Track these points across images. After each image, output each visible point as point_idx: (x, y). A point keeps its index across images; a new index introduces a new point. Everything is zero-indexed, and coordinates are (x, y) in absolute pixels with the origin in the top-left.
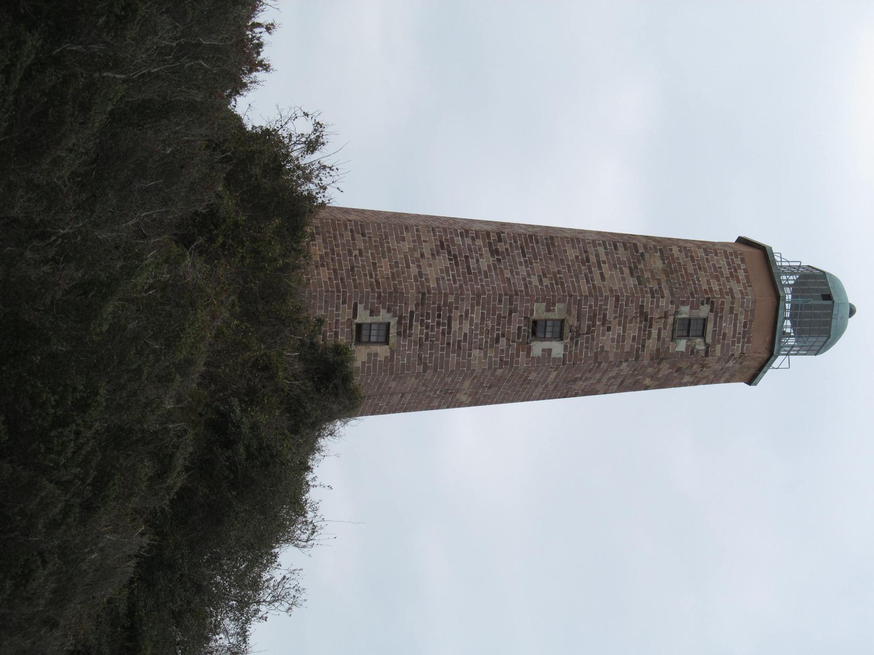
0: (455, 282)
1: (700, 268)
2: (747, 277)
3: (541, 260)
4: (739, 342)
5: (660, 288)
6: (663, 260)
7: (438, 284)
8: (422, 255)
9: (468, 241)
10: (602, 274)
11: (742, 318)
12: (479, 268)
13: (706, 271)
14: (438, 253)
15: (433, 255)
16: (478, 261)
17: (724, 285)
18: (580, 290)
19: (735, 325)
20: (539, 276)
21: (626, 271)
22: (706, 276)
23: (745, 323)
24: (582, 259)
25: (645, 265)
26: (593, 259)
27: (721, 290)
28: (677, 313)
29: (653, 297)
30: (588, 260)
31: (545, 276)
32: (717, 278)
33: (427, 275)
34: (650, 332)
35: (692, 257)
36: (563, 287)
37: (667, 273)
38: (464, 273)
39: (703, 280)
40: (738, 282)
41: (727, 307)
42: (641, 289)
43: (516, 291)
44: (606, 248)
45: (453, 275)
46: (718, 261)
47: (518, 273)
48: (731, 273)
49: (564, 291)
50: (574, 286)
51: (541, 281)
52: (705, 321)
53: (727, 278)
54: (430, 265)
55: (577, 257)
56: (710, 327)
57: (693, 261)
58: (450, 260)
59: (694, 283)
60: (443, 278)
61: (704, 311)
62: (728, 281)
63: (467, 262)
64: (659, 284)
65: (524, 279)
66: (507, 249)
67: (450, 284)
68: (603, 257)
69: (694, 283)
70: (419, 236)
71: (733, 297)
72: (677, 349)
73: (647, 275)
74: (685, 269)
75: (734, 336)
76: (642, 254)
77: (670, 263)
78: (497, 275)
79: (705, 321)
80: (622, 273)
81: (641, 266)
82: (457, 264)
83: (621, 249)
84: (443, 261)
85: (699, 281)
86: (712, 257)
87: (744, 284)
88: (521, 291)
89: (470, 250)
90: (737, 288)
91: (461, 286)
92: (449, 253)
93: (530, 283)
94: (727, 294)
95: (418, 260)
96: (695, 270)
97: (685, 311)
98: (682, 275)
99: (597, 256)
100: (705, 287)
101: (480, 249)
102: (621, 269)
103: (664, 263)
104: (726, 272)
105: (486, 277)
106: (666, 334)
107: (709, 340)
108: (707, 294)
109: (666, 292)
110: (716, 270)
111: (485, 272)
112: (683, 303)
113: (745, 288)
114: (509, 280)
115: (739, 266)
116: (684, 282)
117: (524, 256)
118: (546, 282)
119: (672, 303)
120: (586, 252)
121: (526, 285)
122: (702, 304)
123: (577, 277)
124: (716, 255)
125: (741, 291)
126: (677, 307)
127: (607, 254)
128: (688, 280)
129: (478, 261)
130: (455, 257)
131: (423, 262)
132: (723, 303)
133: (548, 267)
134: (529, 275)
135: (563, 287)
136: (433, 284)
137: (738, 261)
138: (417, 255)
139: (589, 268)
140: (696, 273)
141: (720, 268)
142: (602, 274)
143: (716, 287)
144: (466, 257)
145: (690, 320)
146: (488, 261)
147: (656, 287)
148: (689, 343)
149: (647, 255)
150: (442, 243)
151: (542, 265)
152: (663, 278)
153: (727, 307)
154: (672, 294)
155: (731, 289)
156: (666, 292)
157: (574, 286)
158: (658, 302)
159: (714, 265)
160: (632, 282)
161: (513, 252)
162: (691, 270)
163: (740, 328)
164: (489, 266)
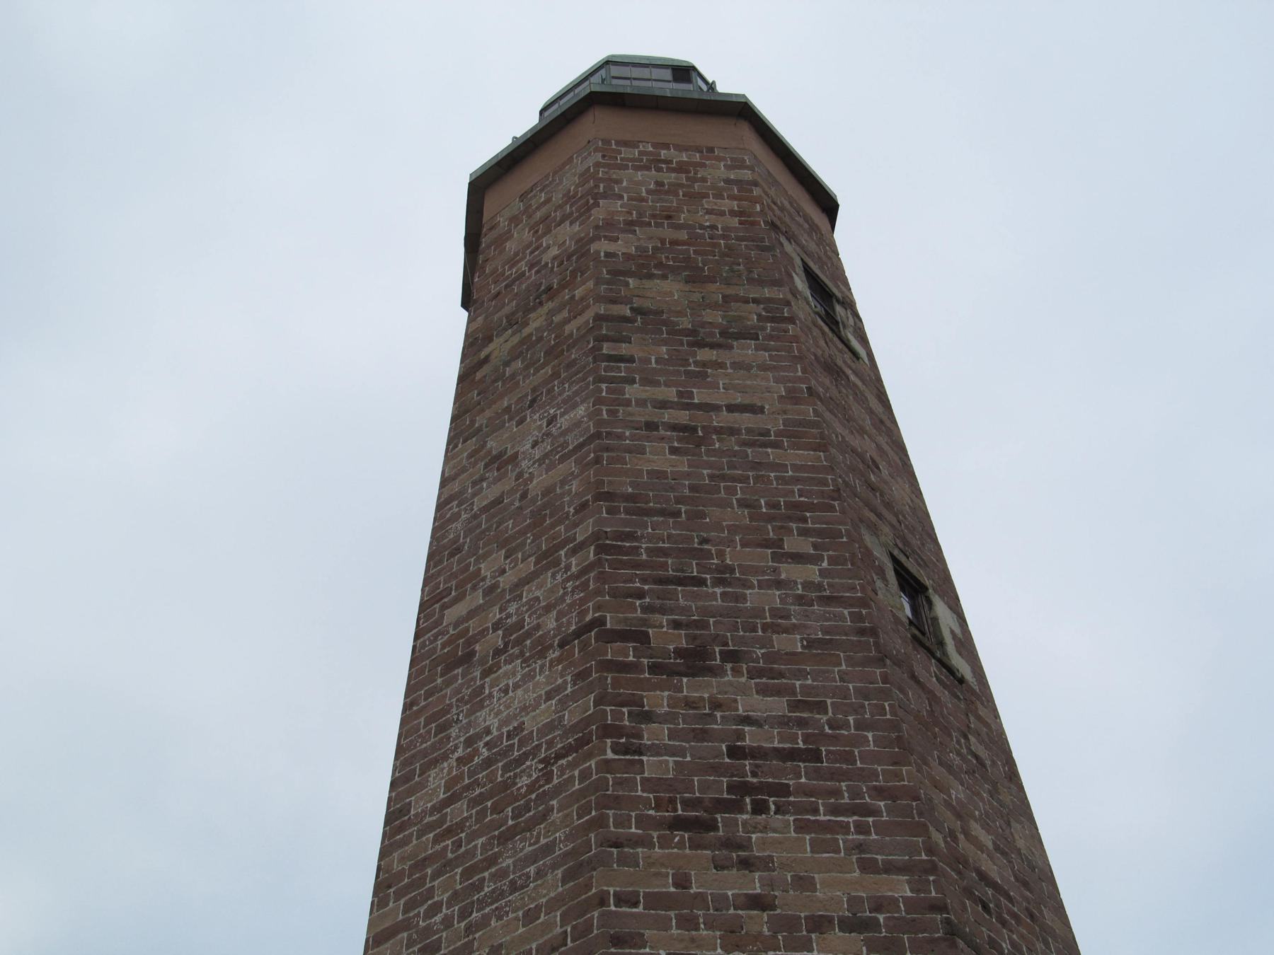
0: (875, 812)
1: (669, 217)
2: (679, 148)
3: (704, 541)
5: (755, 301)
6: (650, 276)
7: (889, 868)
8: (757, 903)
9: (652, 734)
10: (731, 408)
11: (786, 203)
12: (783, 722)
13: (679, 210)
14: (743, 845)
15: (746, 864)
16: (747, 720)
18: (813, 469)
20: (777, 557)
21: (705, 354)
24: (680, 440)
25: (680, 313)
26: (683, 417)
27: (732, 198)
29: (791, 320)
30: (688, 429)
31: (778, 543)
32: (695, 197)
33: (853, 901)
35: (631, 223)
36: (811, 507)
38: (817, 774)
42: (771, 337)
43: (862, 632)
44: (633, 381)
45: (835, 810)
46: (639, 183)
47: (775, 613)
48: (670, 170)
49: (832, 509)
50: (797, 480)
51: (798, 558)
54: (803, 883)
55: (674, 451)
57: (649, 224)
58: (760, 808)
60: (860, 847)
63: (755, 753)
64: (746, 301)
65: (800, 600)
66: (677, 625)
67: (880, 829)
68: (671, 394)
70: (656, 901)
74: (674, 243)
77: (660, 265)
78: (802, 674)
80: (722, 365)
81: (685, 323)
82: (783, 790)
83: (624, 349)
84: (774, 836)
85: (713, 227)
86: (626, 190)
88: (857, 617)
89: (702, 735)
90: (718, 172)
91: (880, 792)
92: (737, 807)
93: (808, 585)
95: (790, 924)
96: (679, 227)
99: (663, 405)
101: (690, 704)
102: (704, 364)
103: (664, 277)
104: (669, 178)
105: (821, 707)
109: (767, 292)
111: (795, 706)
113: (719, 159)
114: (811, 644)
115: (641, 153)
117: (701, 582)
118: (793, 543)
120: (651, 426)
121: (828, 600)
123: (756, 466)
124: (619, 182)
127: (648, 381)
129: (747, 720)
130: (742, 789)
131: (791, 903)
133: (733, 529)
134: (779, 584)
135: (811, 507)
136: (902, 889)
138: (759, 922)
139: (719, 431)
142: (731, 408)
143: (727, 204)
144: (734, 752)
146: (743, 690)
149: (637, 303)
150: (678, 824)
151: (731, 543)
152: (716, 291)
155: (727, 181)
156: (767, 292)
157: (797, 480)
159: (649, 192)
160: (746, 351)
161: (685, 610)
162: (683, 235)
164: (764, 691)
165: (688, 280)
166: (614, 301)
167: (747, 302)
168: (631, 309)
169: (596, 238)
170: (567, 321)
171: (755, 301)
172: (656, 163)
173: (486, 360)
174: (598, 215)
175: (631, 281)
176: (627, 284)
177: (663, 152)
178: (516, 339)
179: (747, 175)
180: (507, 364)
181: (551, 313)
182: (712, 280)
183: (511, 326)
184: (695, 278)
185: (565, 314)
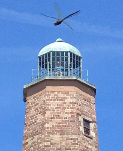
1: (58, 116)
4: (90, 105)
5: (72, 139)
6: (54, 134)
17: (69, 106)
19: (85, 105)
22: (63, 113)
23: (84, 99)
25: (59, 144)
27: (71, 108)
28: (82, 133)
29: (77, 144)
32: (64, 109)
34: (90, 148)
37: (62, 134)
39: (66, 116)
40: (66, 98)
41: (79, 107)
46: (54, 105)
52: (85, 120)
53: (64, 103)
56: (87, 118)
57: (55, 118)
59: (68, 121)
61: (81, 119)
62: (66, 103)
69: (68, 121)
71: (75, 103)
72: (95, 137)
73: (64, 144)
74: (59, 123)
75: (89, 107)
76: (52, 144)
79: (85, 120)
85: (66, 118)
87: (67, 95)
90: (69, 100)
94: (74, 106)
96: (60, 118)
97: (82, 129)
98: (63, 126)
100: (70, 116)
103: (57, 134)
104: (60, 103)
106: (90, 141)
107: (91, 120)
108: (74, 116)
110: (59, 108)
112: (79, 129)
113: (69, 95)
116: (68, 126)
119: (79, 135)
122: (79, 119)
125: (71, 98)
126: (80, 132)
128: (66, 123)
132: (78, 109)
137: (53, 95)
140: (62, 118)
141: (58, 105)
143: (70, 110)
145: (84, 127)
147: (72, 141)
148: (92, 130)
153: (79, 107)
154: (75, 134)
155: (70, 103)
156: (74, 137)
158: (79, 142)
162: (60, 121)
163: (86, 103)
165: (61, 134)
166: (48, 142)
167: (70, 140)
168: (51, 143)
169: (45, 123)
170: (40, 143)
171: (72, 139)
172: (57, 99)
173: (27, 143)
174: (46, 116)
175: (51, 135)
176: (50, 136)
177: (59, 94)
178: (31, 142)
179: (74, 100)
180: (31, 147)
181: (38, 139)
182: (64, 134)
183: (31, 136)
184: (62, 134)
185: (39, 141)
